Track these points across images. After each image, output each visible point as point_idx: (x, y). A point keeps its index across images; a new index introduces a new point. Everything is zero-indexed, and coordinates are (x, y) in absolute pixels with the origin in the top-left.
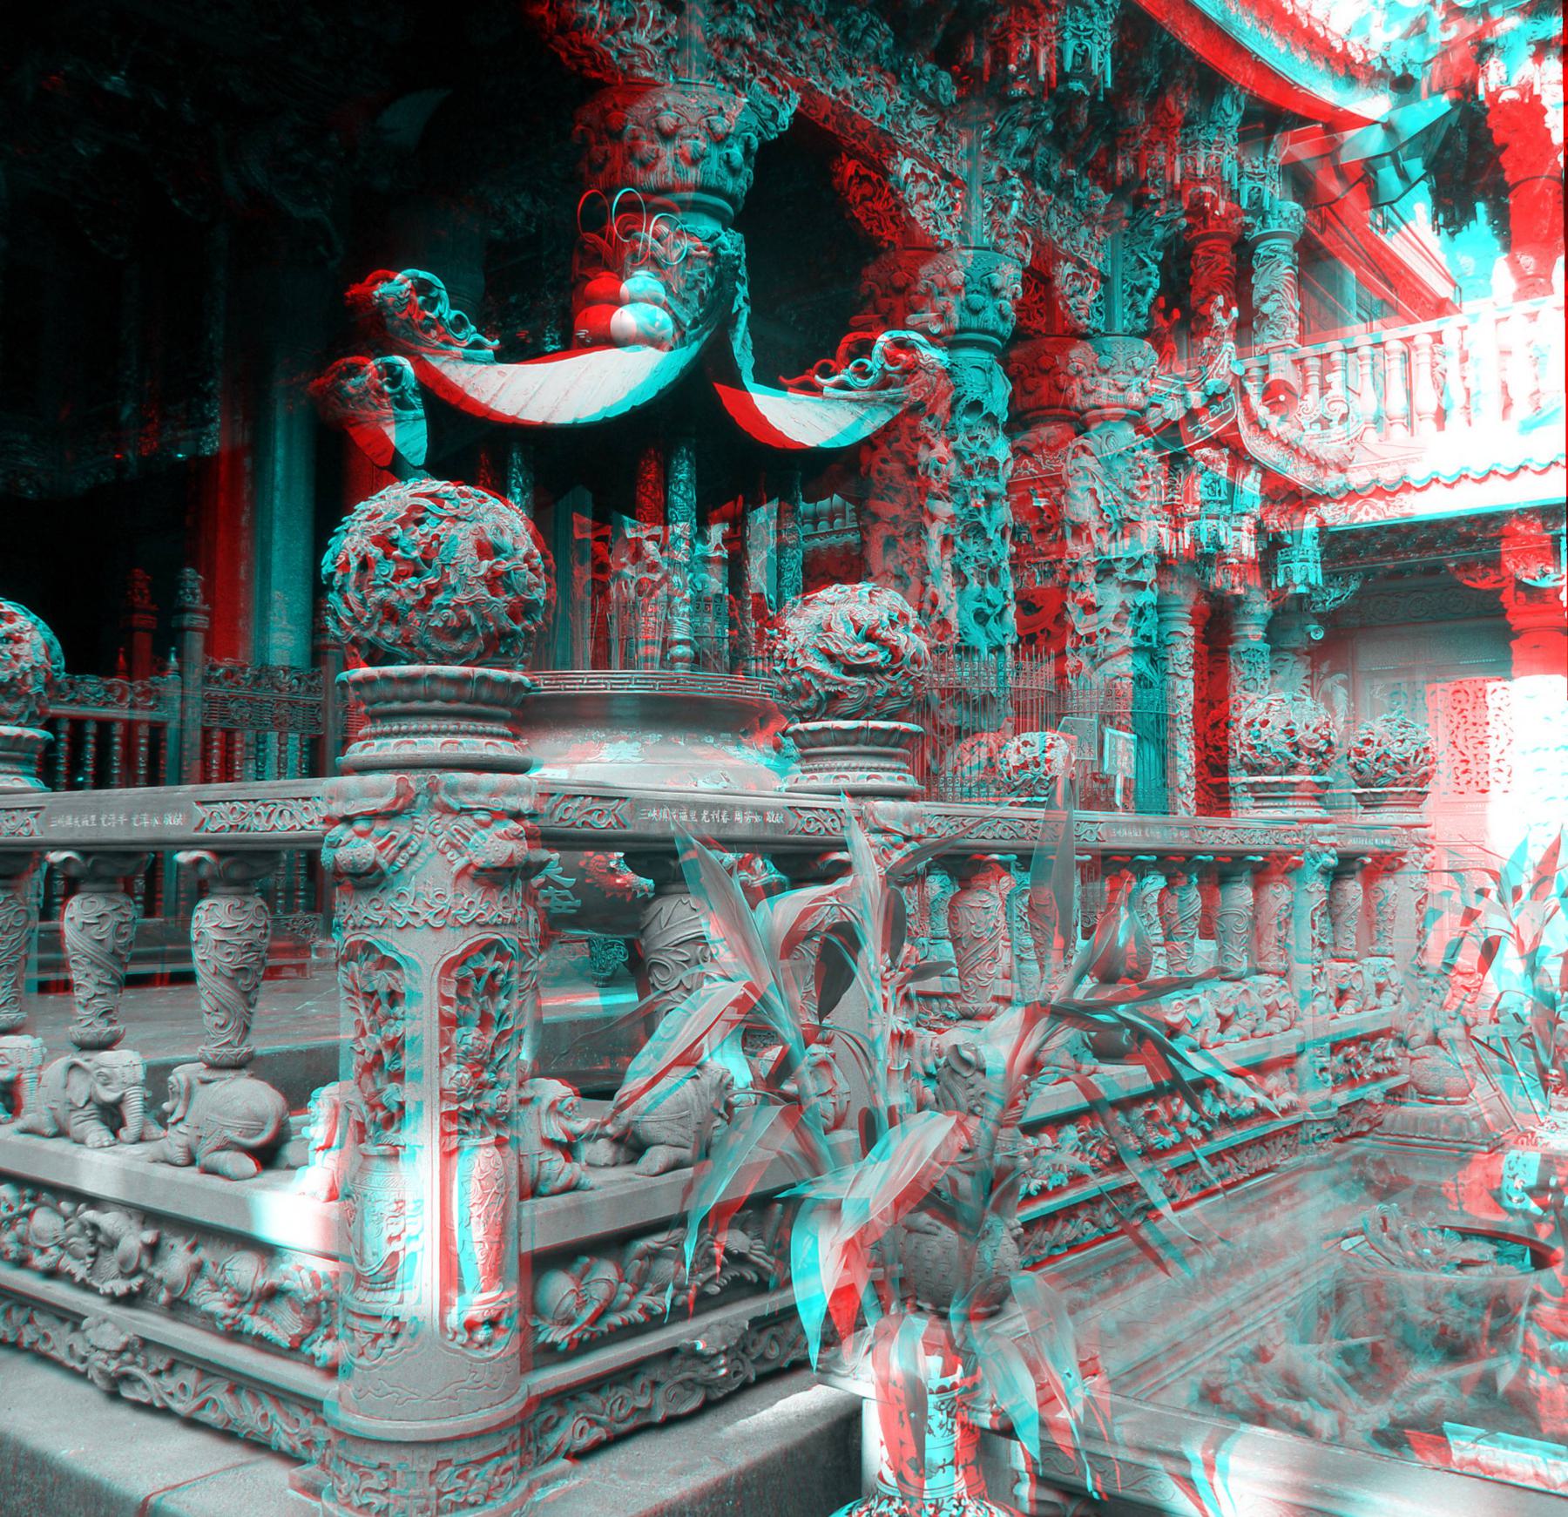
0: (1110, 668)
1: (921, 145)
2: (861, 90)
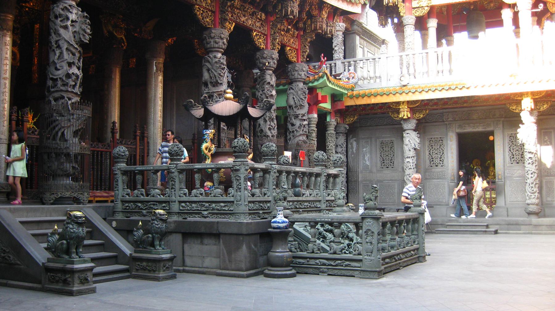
0: (297, 139)
1: (258, 29)
2: (247, 20)
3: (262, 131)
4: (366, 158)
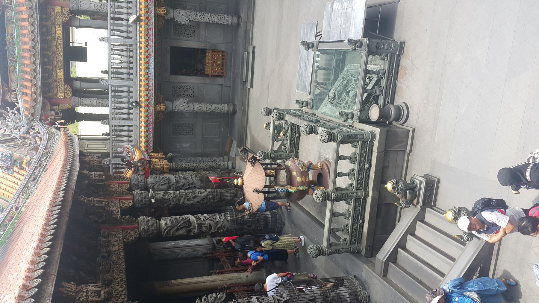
0: (195, 181)
3: (203, 200)
4: (185, 146)
